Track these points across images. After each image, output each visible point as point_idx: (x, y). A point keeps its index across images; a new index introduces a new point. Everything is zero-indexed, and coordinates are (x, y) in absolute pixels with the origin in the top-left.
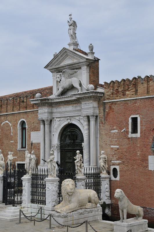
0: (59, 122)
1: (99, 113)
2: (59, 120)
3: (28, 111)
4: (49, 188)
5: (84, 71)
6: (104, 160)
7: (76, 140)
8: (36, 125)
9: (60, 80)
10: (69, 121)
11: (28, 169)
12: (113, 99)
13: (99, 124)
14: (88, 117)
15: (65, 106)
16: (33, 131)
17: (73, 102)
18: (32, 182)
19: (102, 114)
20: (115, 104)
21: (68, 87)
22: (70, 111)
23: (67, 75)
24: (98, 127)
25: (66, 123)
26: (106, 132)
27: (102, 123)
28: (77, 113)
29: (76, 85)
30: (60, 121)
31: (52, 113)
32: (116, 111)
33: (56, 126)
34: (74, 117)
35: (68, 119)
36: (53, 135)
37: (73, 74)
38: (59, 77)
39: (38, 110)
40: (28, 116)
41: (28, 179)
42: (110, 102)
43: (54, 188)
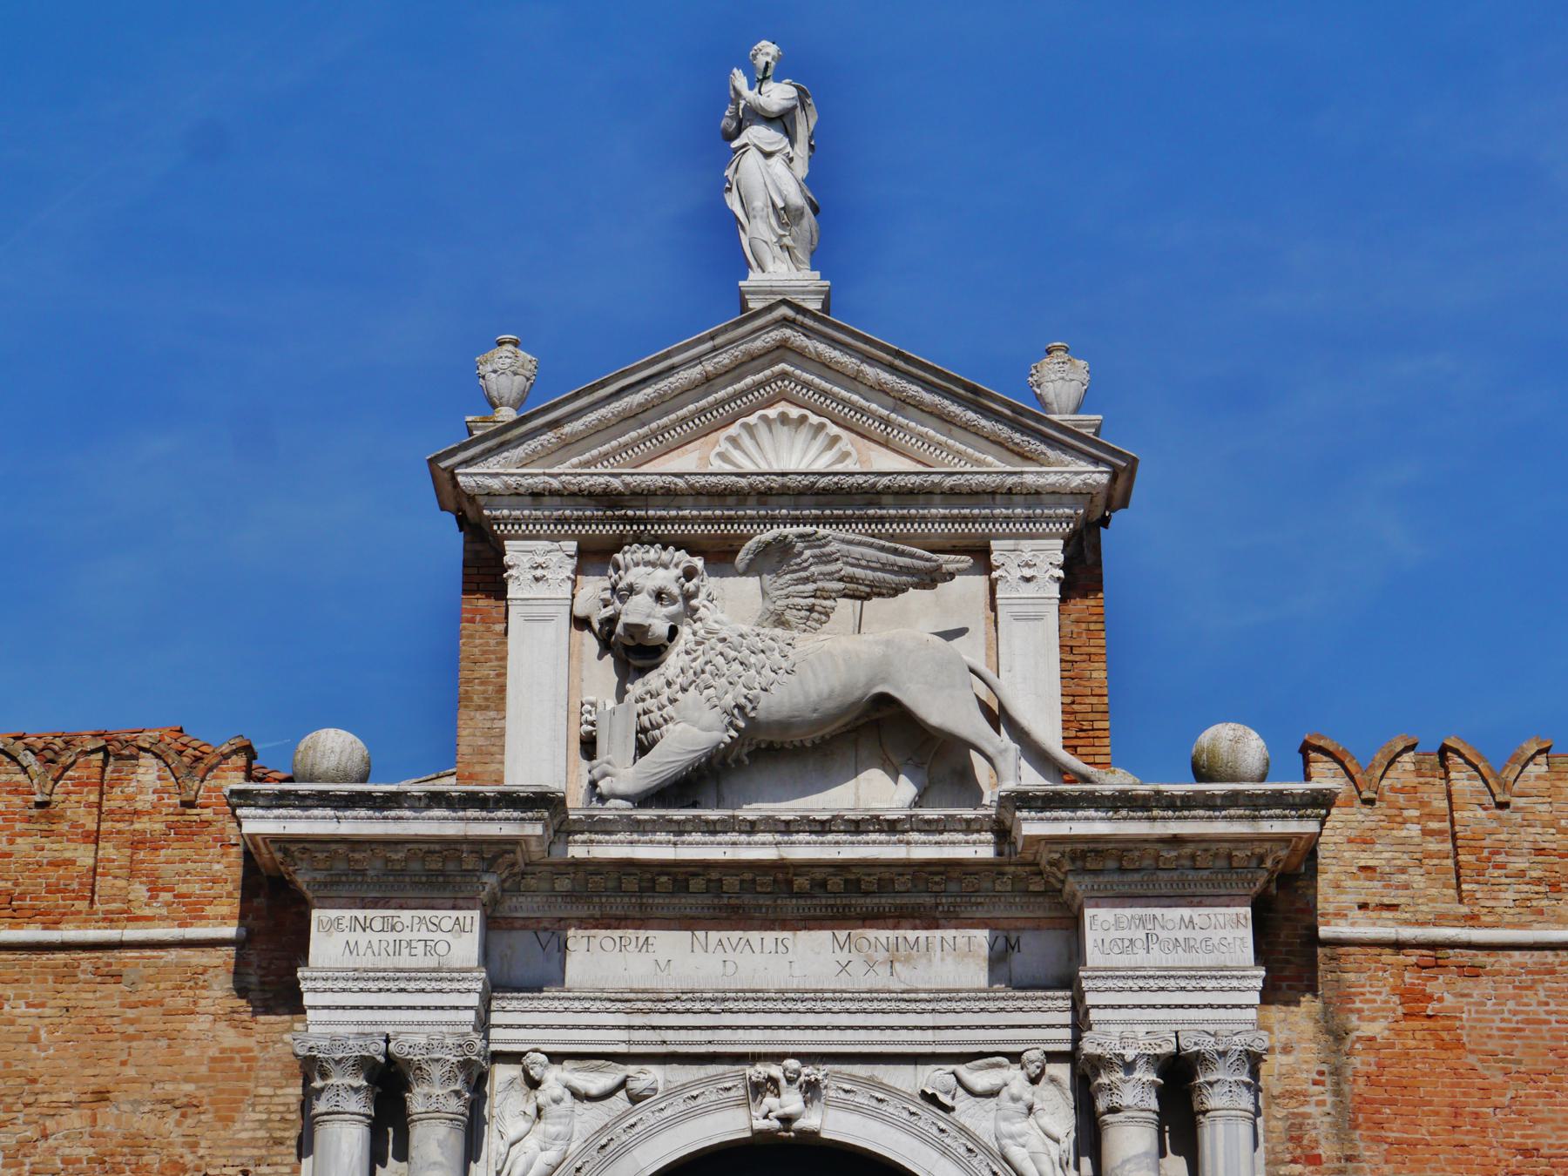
0: (591, 1117)
2: (597, 1080)
5: (1028, 590)
8: (144, 1123)
9: (673, 632)
10: (791, 1101)
12: (1439, 920)
14: (1178, 1078)
17: (884, 886)
20: (1474, 972)
21: (785, 725)
22: (790, 998)
23: (811, 587)
25: (729, 1124)
27: (1315, 1160)
28: (927, 1020)
29: (946, 708)
30: (620, 1101)
32: (1490, 1046)
37: (896, 591)
38: (675, 590)
42: (1398, 946)
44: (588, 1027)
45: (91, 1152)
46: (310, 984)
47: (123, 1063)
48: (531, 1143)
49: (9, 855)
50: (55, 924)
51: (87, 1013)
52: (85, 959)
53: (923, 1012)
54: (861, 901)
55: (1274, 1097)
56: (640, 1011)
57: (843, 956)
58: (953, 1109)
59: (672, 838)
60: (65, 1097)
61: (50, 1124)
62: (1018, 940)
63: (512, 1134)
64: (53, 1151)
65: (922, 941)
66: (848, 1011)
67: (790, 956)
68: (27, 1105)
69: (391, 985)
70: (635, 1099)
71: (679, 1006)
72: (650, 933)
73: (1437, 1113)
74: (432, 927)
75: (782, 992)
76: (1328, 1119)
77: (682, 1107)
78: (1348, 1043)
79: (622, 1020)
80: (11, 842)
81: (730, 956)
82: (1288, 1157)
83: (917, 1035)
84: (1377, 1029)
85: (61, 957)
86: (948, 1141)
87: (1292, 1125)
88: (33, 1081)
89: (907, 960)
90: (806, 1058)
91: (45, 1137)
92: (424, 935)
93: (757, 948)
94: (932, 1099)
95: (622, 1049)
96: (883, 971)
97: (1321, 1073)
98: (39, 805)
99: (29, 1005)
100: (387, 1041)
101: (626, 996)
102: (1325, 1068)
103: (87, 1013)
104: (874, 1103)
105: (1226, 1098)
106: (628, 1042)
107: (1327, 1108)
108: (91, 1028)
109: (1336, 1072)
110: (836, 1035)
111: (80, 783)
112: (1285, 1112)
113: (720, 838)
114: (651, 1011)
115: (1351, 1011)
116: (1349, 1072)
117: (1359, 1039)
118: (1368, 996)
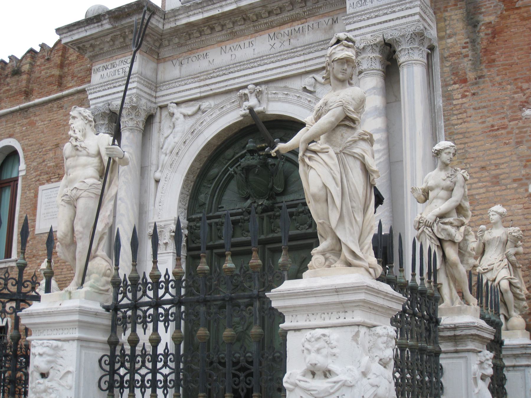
0: (191, 121)
1: (441, 38)
2: (189, 110)
3: (37, 101)
4: (327, 373)
6: (511, 250)
7: (283, 194)
11: (82, 246)
13: (445, 85)
15: (234, 44)
16: (49, 181)
18: (113, 343)
19: (458, 39)
24: (439, 102)
26: (490, 121)
27: (465, 81)
28: (302, 58)
31: (154, 85)
33: (171, 142)
34: (281, 84)
35: (245, 97)
36: (157, 181)
39: (84, 91)
40: (32, 124)
41: (82, 312)
43: (376, 367)
44: (187, 90)
45: (54, 164)
46: (90, 92)
47: (63, 134)
48: (171, 136)
49: (39, 77)
50: (50, 95)
51: (55, 121)
52: (55, 105)
53: (300, 55)
54: (275, 18)
55: (445, 58)
56: (203, 80)
57: (272, 42)
58: (315, 92)
59: (200, 10)
60: (49, 148)
61: (45, 157)
62: (337, 19)
63: (165, 135)
64: (46, 165)
65: (301, 29)
66: (273, 62)
67: (254, 47)
68: (40, 152)
69: (112, 86)
70: (204, 112)
71: (215, 75)
72: (207, 51)
73: (522, 49)
74: (125, 63)
75: (249, 60)
76: (470, 62)
77: (218, 113)
78: (479, 27)
79: (197, 84)
80: (41, 73)
81: (234, 52)
82: (452, 82)
83: (299, 65)
84: (491, 18)
85: (50, 105)
86: (312, 105)
87: (453, 68)
88: (42, 144)
89: (296, 37)
90: (256, 84)
91: (44, 161)
92: (123, 66)
93: (242, 47)
94: (305, 89)
95: (198, 95)
96: (286, 43)
97: (466, 43)
98: (48, 59)
99: (42, 121)
100: (109, 105)
101: (197, 75)
102: (468, 40)
103: (55, 121)
104: (285, 96)
105: (406, 57)
106: (200, 92)
107: (470, 58)
108: (56, 125)
109: (473, 41)
110: (269, 73)
111: (58, 50)
112: (449, 64)
113: (215, 6)
114: (206, 79)
115: (481, 13)
116: (479, 40)
117: (483, 24)
118: (488, 5)
